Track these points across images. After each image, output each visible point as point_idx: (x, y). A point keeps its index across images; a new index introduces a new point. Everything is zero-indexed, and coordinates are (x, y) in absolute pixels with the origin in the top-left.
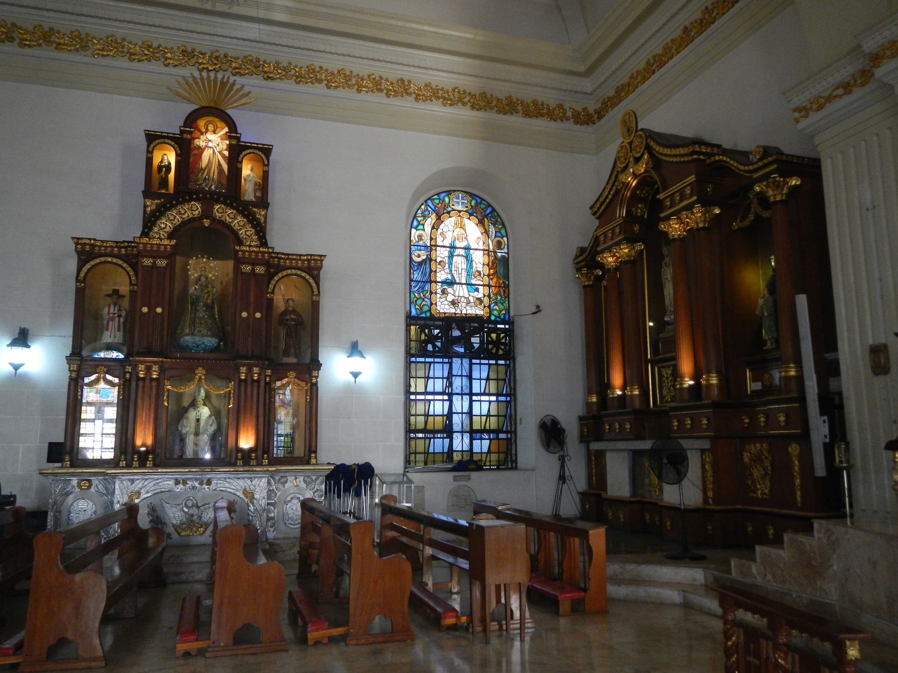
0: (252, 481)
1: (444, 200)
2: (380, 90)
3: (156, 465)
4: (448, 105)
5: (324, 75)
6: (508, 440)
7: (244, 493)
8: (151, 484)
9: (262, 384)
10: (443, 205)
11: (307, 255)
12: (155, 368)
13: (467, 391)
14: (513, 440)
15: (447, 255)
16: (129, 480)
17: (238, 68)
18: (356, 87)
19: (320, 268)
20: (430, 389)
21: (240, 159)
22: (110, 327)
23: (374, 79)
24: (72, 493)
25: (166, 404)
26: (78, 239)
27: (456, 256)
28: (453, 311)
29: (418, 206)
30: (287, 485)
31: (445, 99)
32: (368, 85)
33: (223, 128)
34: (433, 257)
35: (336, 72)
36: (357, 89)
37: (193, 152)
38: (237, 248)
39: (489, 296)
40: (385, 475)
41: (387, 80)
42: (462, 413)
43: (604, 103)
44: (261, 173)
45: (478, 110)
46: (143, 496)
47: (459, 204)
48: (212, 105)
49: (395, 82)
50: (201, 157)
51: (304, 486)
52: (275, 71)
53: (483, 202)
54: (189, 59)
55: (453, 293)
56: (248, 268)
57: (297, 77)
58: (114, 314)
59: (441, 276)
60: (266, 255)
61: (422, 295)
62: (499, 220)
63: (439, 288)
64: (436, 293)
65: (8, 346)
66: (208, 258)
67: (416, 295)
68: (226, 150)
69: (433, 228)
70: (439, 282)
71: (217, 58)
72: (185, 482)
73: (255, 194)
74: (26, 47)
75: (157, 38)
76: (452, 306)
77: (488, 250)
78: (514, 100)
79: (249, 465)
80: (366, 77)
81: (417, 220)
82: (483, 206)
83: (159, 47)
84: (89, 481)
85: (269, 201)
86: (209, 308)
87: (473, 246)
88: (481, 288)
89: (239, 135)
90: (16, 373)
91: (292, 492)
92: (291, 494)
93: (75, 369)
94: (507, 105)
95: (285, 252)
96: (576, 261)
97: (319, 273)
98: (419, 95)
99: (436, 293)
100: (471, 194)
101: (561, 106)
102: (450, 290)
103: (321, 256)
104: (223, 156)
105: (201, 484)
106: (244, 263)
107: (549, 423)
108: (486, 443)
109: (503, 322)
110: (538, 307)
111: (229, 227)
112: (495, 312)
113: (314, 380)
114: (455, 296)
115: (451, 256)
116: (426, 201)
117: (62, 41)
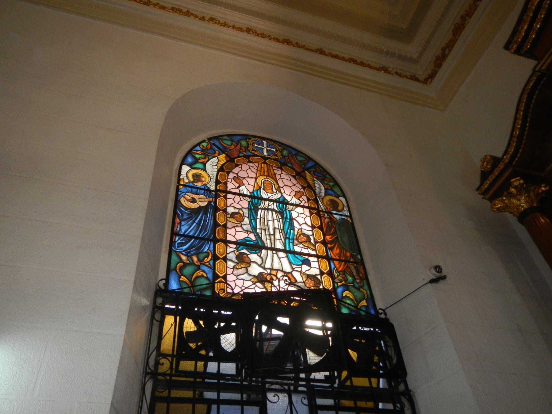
27: (262, 209)
29: (196, 142)
39: (330, 273)
53: (300, 154)
61: (195, 259)
62: (328, 176)
64: (225, 259)
67: (184, 258)
69: (221, 169)
81: (194, 157)
82: (300, 158)
102: (254, 257)
110: (438, 268)
114: (265, 268)
115: (253, 209)
116: (210, 139)
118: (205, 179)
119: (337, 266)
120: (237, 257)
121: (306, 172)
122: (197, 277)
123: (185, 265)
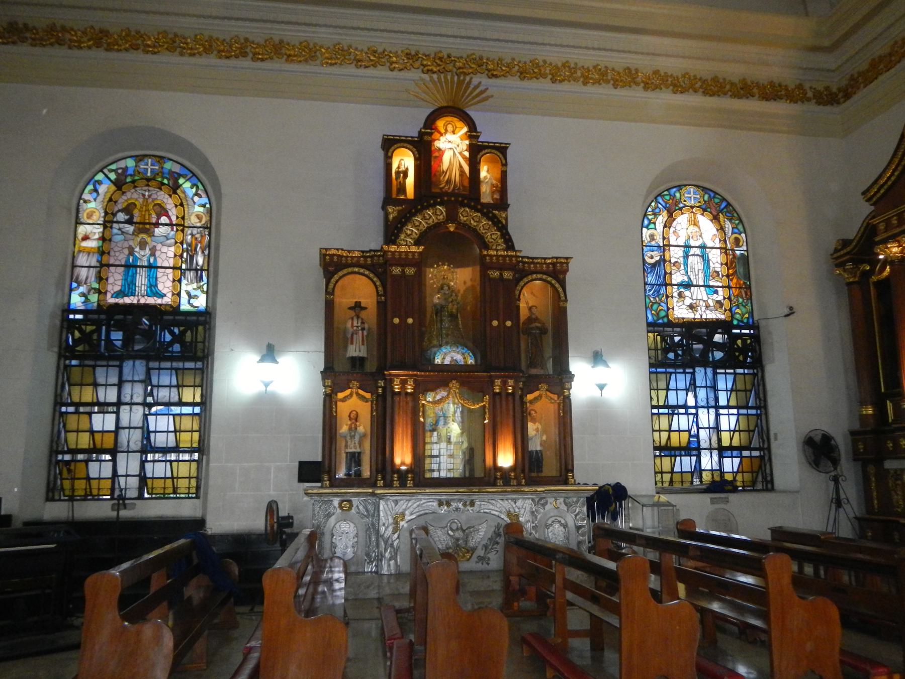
0: (515, 503)
1: (674, 195)
2: (608, 82)
3: (417, 485)
5: (548, 69)
6: (761, 458)
8: (415, 505)
9: (517, 398)
10: (674, 201)
11: (553, 258)
12: (411, 382)
13: (712, 403)
14: (767, 458)
15: (682, 255)
16: (512, 499)
17: (462, 68)
18: (582, 79)
19: (567, 270)
20: (672, 401)
21: (478, 160)
22: (355, 340)
23: (600, 70)
24: (333, 514)
25: (422, 419)
26: (327, 250)
27: (691, 255)
29: (648, 204)
30: (548, 507)
32: (593, 76)
33: (462, 128)
34: (667, 258)
35: (560, 65)
36: (583, 82)
37: (434, 155)
38: (485, 253)
39: (729, 298)
40: (636, 496)
41: (613, 70)
42: (709, 428)
43: (852, 78)
44: (499, 176)
45: (711, 96)
46: (408, 518)
47: (691, 196)
48: (451, 104)
49: (621, 71)
50: (442, 159)
51: (565, 508)
52: (499, 68)
53: (717, 196)
54: (414, 62)
55: (690, 296)
56: (495, 274)
57: (521, 73)
58: (357, 327)
59: (677, 278)
60: (514, 259)
61: (657, 299)
62: (735, 215)
63: (675, 291)
64: (672, 297)
65: (258, 362)
66: (448, 266)
67: (652, 299)
68: (466, 150)
69: (665, 226)
71: (441, 59)
72: (448, 504)
73: (492, 197)
74: (259, 61)
75: (382, 43)
76: (690, 310)
77: (725, 249)
78: (749, 83)
79: (510, 485)
80: (591, 68)
81: (648, 219)
82: (717, 201)
83: (384, 52)
84: (350, 501)
85: (509, 203)
86: (453, 317)
87: (709, 244)
88: (720, 290)
89: (478, 134)
90: (266, 390)
91: (552, 514)
92: (551, 517)
93: (330, 384)
94: (742, 89)
95: (530, 256)
96: (835, 256)
97: (565, 277)
98: (648, 84)
99: (672, 297)
100: (702, 187)
101: (800, 87)
102: (687, 293)
103: (567, 258)
104: (464, 157)
105: (465, 505)
106: (491, 268)
107: (818, 438)
108: (737, 461)
109: (747, 327)
110: (791, 308)
111: (474, 231)
112: (738, 316)
113: (566, 394)
114: (693, 300)
115: (686, 256)
116: (656, 198)
117: (292, 53)
119: (734, 292)
121: (720, 214)
122: (660, 310)
123: (653, 304)
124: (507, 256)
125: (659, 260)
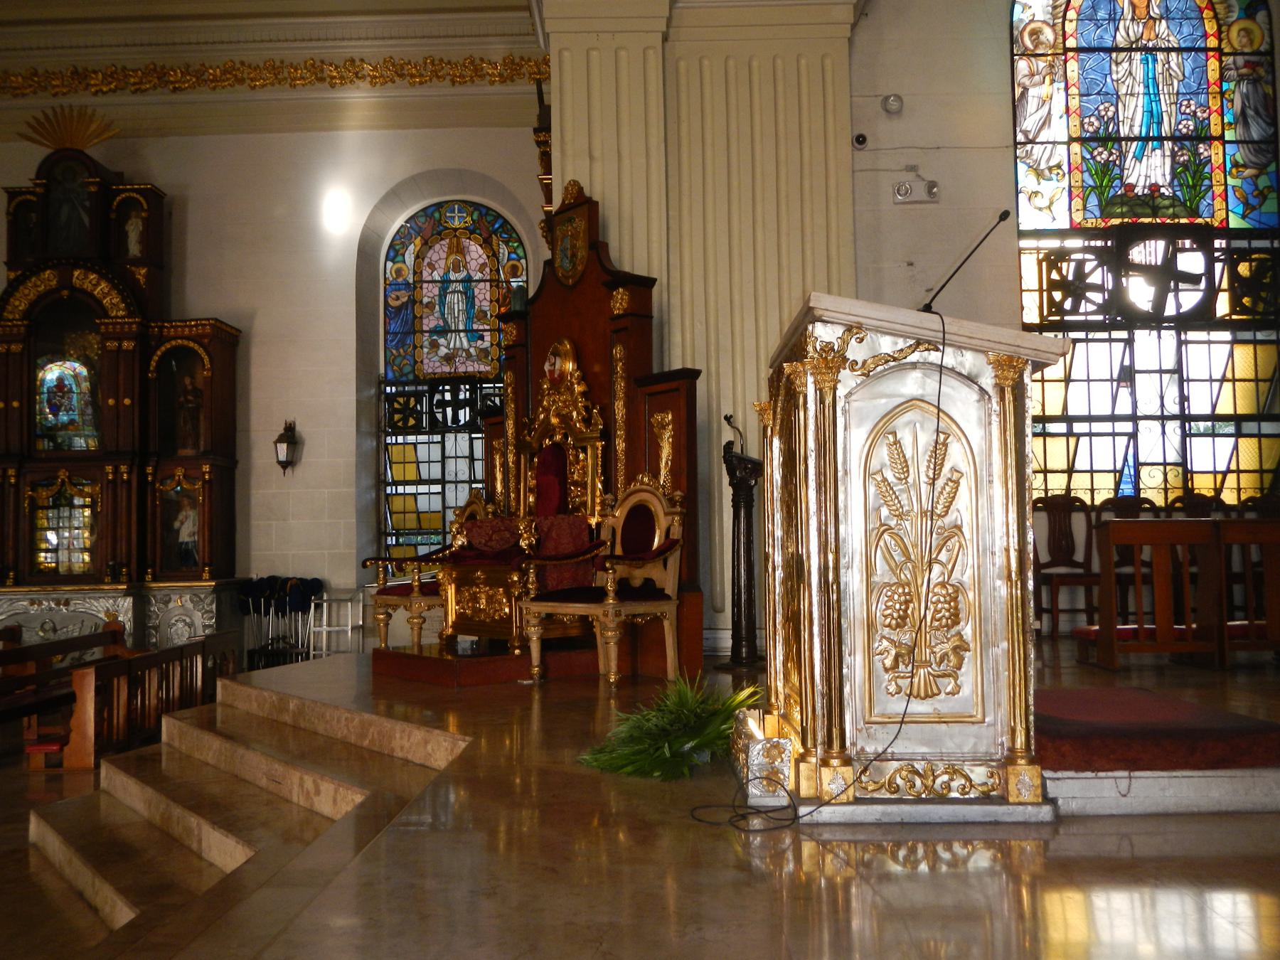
4: (417, 85)
7: (106, 615)
15: (437, 293)
28: (447, 369)
30: (171, 605)
31: (412, 76)
34: (417, 298)
51: (190, 605)
55: (446, 344)
56: (112, 345)
59: (430, 323)
61: (401, 351)
62: (514, 235)
67: (394, 352)
69: (417, 257)
70: (426, 332)
77: (498, 281)
82: (490, 218)
91: (177, 613)
102: (442, 341)
118: (405, 272)
120: (430, 344)
124: (125, 323)
125: (407, 302)
